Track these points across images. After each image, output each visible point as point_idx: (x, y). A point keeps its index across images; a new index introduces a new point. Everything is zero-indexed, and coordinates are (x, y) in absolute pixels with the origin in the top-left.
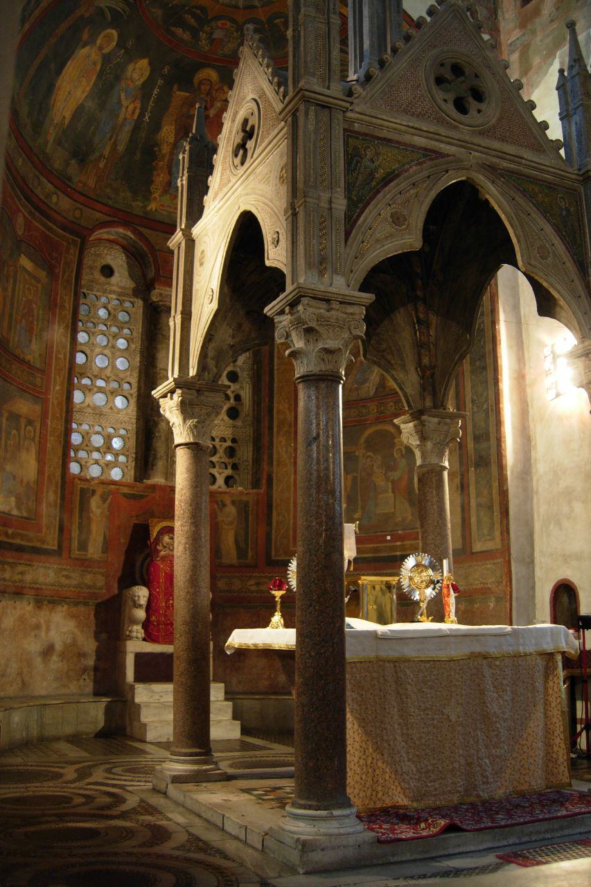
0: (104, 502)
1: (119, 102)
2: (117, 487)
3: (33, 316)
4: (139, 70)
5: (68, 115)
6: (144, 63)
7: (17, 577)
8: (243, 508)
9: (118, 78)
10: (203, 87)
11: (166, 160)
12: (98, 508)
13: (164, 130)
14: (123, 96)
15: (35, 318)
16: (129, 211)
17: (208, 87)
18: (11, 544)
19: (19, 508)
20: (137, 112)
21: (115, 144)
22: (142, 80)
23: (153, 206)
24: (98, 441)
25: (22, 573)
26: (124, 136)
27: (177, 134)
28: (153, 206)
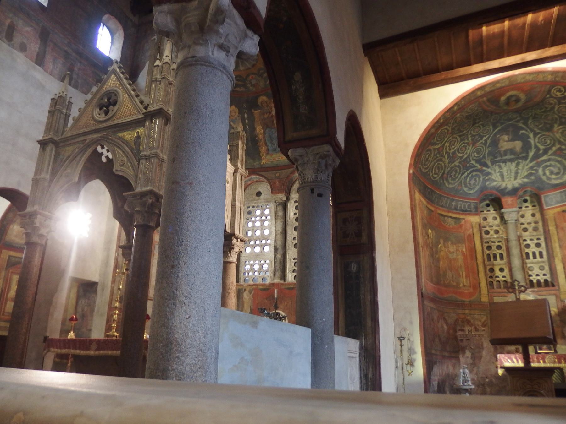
0: (250, 293)
2: (257, 286)
10: (264, 105)
11: (263, 141)
13: (257, 129)
16: (254, 167)
17: (266, 104)
22: (237, 114)
23: (263, 162)
24: (256, 267)
27: (263, 128)
28: (263, 162)
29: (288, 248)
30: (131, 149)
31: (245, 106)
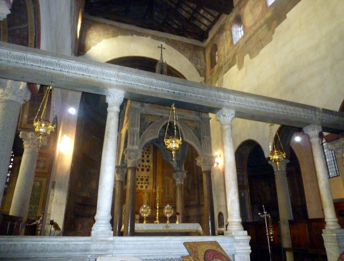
8: (149, 194)
30: (195, 133)
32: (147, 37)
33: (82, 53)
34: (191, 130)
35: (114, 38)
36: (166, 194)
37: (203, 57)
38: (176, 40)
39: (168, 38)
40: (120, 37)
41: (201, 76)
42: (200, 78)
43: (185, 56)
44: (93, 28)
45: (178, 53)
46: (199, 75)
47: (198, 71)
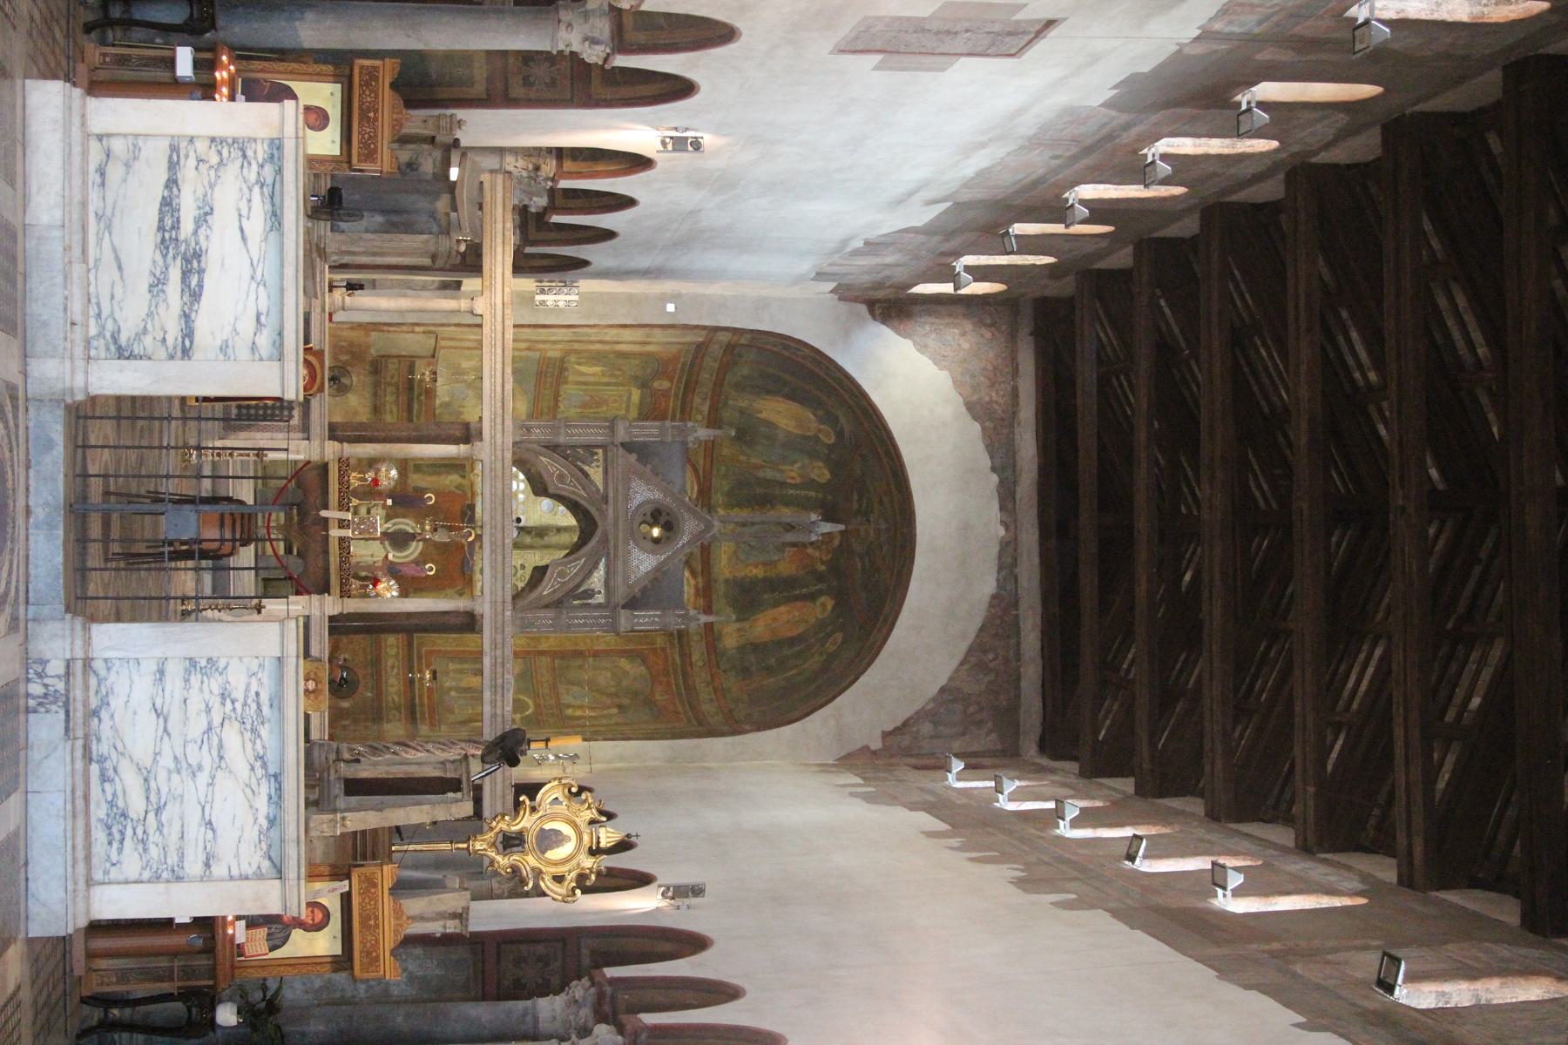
1: (794, 462)
3: (597, 407)
4: (821, 473)
5: (764, 415)
6: (828, 476)
7: (388, 407)
9: (813, 455)
12: (451, 481)
14: (799, 464)
15: (596, 410)
18: (413, 399)
19: (441, 405)
20: (792, 482)
21: (762, 467)
25: (391, 412)
26: (769, 474)
29: (545, 551)
31: (830, 497)
32: (1002, 522)
33: (878, 312)
34: (577, 580)
35: (964, 409)
36: (458, 666)
37: (974, 748)
38: (1018, 633)
39: (1023, 605)
40: (977, 427)
41: (885, 735)
42: (878, 734)
43: (957, 670)
44: (988, 335)
45: (964, 646)
46: (889, 727)
47: (905, 724)
